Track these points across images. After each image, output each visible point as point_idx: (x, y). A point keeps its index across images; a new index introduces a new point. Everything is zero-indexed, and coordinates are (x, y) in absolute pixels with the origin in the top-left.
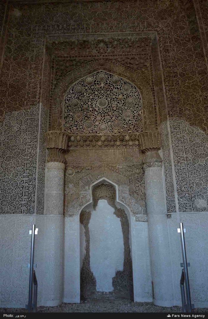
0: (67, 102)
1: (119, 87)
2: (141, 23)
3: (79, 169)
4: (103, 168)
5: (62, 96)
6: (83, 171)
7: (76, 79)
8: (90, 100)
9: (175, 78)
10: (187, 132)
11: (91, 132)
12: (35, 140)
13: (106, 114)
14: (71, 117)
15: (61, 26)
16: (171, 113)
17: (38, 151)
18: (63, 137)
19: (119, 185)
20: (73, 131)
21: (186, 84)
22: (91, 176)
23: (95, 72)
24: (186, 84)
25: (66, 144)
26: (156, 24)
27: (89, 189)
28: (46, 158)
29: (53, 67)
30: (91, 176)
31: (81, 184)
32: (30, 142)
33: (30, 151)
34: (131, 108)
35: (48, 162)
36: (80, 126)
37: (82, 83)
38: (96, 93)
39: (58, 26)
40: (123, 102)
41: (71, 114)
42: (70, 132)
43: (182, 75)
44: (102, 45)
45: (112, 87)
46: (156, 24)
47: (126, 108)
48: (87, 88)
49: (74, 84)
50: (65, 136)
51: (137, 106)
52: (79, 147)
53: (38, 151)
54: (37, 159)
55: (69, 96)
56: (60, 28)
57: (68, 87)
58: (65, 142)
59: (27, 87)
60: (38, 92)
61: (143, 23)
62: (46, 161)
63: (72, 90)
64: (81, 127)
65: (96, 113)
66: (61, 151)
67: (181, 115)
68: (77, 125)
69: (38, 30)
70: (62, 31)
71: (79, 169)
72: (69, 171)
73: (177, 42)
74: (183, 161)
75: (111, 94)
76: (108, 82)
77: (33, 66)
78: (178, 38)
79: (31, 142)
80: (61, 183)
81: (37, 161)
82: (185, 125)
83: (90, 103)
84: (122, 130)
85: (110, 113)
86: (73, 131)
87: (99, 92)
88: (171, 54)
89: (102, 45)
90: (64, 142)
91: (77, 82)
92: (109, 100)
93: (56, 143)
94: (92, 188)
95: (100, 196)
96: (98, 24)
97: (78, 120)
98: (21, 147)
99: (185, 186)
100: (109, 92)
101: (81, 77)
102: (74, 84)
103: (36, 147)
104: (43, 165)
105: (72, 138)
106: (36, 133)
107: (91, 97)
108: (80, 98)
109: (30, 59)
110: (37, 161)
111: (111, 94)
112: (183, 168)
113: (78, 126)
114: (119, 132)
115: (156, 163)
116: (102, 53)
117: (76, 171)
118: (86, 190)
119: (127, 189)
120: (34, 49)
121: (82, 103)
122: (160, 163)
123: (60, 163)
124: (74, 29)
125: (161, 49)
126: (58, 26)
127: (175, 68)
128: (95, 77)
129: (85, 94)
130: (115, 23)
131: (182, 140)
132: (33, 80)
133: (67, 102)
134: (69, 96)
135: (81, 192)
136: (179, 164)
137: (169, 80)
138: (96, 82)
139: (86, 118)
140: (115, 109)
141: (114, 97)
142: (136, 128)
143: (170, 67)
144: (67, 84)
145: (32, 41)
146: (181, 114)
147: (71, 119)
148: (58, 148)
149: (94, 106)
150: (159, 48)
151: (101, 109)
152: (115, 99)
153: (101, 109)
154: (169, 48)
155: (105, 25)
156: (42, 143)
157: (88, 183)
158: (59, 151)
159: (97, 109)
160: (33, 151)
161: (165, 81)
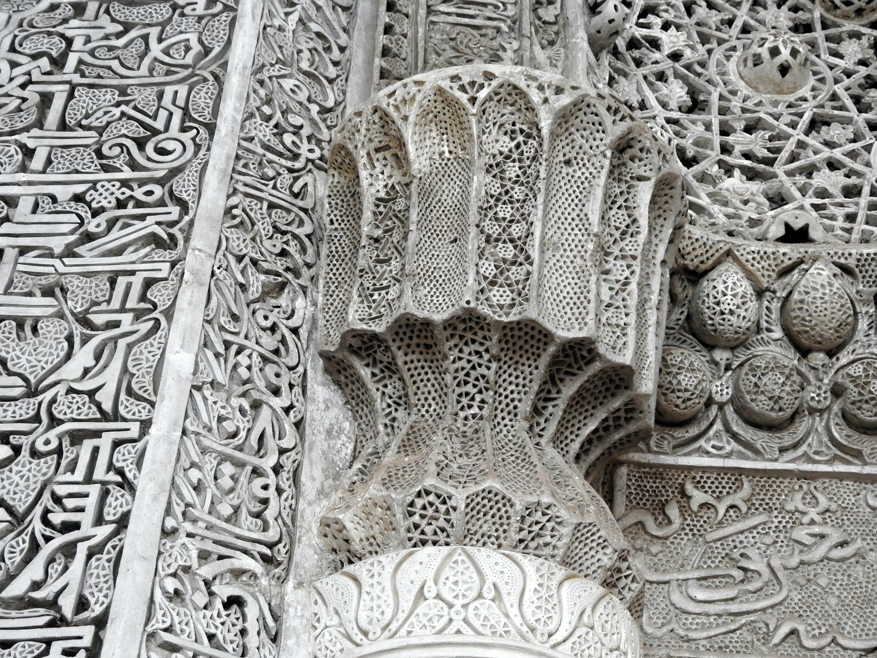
12: (149, 226)
14: (677, 75)
17: (180, 361)
18: (609, 201)
20: (715, 209)
25: (652, 317)
28: (311, 514)
32: (58, 245)
35: (344, 554)
36: (809, 171)
50: (644, 193)
52: (815, 432)
53: (180, 361)
54: (151, 484)
58: (644, 286)
62: (308, 550)
66: (580, 403)
68: (770, 162)
79: (69, 252)
81: (146, 512)
86: (715, 209)
93: (509, 252)
97: (768, 105)
103: (154, 315)
104: (234, 602)
113: (779, 169)
148: (525, 337)
156: (257, 282)
158: (537, 411)
160: (84, 357)
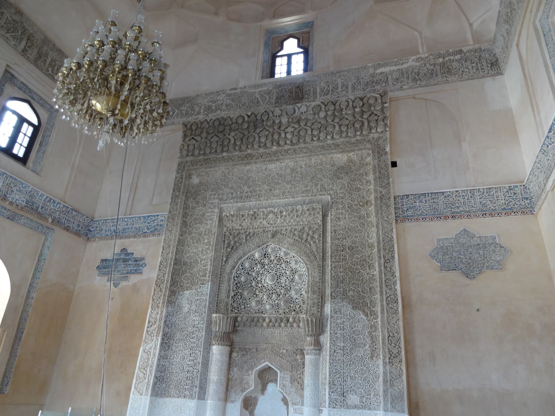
0: (236, 279)
1: (288, 261)
2: (314, 186)
3: (245, 351)
4: (267, 351)
5: (231, 273)
6: (249, 353)
7: (244, 254)
8: (260, 275)
9: (343, 253)
10: (348, 316)
11: (257, 311)
13: (274, 291)
15: (235, 193)
16: (333, 294)
19: (281, 371)
21: (354, 259)
22: (255, 360)
23: (265, 246)
24: (354, 259)
26: (330, 187)
27: (252, 374)
29: (224, 241)
30: (255, 360)
31: (246, 367)
33: (197, 333)
34: (299, 285)
37: (252, 258)
38: (266, 267)
39: (232, 194)
40: (292, 277)
41: (240, 291)
42: (237, 312)
43: (351, 248)
44: (271, 216)
45: (282, 261)
46: (330, 187)
47: (294, 284)
48: (257, 262)
49: (243, 259)
51: (304, 283)
55: (239, 272)
56: (234, 196)
57: (237, 262)
59: (199, 265)
60: (209, 269)
61: (316, 186)
63: (242, 266)
64: (249, 306)
65: (265, 290)
67: (344, 297)
69: (214, 198)
70: (236, 200)
71: (245, 351)
72: (234, 355)
73: (350, 208)
74: (339, 351)
75: (281, 268)
76: (278, 255)
77: (206, 241)
78: (352, 203)
80: (224, 368)
82: (347, 309)
83: (259, 279)
84: (287, 310)
85: (278, 290)
87: (269, 266)
88: (342, 223)
89: (271, 216)
90: (228, 325)
91: (246, 257)
92: (279, 275)
94: (255, 372)
95: (269, 380)
96: (271, 190)
98: (190, 329)
99: (339, 379)
100: (278, 266)
101: (249, 252)
102: (243, 259)
105: (239, 319)
106: (204, 314)
107: (261, 272)
108: (250, 273)
109: (203, 233)
110: (203, 344)
111: (281, 268)
112: (339, 358)
114: (284, 313)
115: (313, 351)
116: (272, 224)
117: (242, 354)
118: (249, 375)
119: (288, 377)
120: (208, 222)
121: (252, 279)
122: (318, 351)
123: (224, 347)
124: (247, 196)
125: (333, 217)
126: (232, 194)
127: (344, 241)
128: (265, 250)
129: (255, 269)
130: (289, 186)
131: (342, 326)
132: (205, 257)
133: (236, 279)
134: (239, 272)
135: (245, 377)
136: (335, 354)
137: (336, 256)
138: (266, 256)
139: (255, 296)
140: (283, 285)
141: (283, 271)
142: (301, 308)
143: (339, 239)
144: (236, 261)
145: (207, 212)
146: (345, 296)
147: (240, 297)
149: (263, 281)
150: (330, 215)
151: (270, 286)
152: (284, 275)
153: (270, 286)
154: (341, 216)
155: (277, 191)
157: (252, 368)
159: (265, 285)
161: (331, 256)
